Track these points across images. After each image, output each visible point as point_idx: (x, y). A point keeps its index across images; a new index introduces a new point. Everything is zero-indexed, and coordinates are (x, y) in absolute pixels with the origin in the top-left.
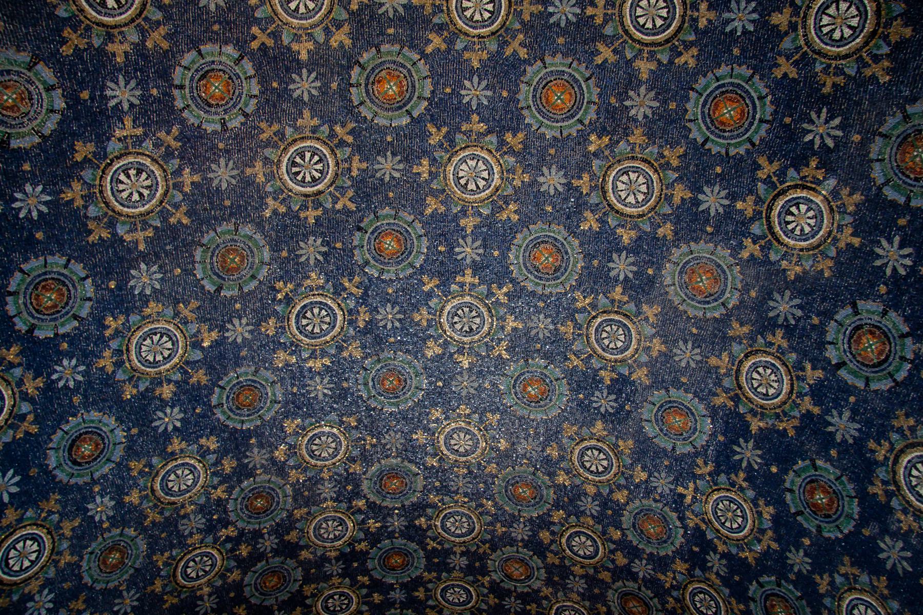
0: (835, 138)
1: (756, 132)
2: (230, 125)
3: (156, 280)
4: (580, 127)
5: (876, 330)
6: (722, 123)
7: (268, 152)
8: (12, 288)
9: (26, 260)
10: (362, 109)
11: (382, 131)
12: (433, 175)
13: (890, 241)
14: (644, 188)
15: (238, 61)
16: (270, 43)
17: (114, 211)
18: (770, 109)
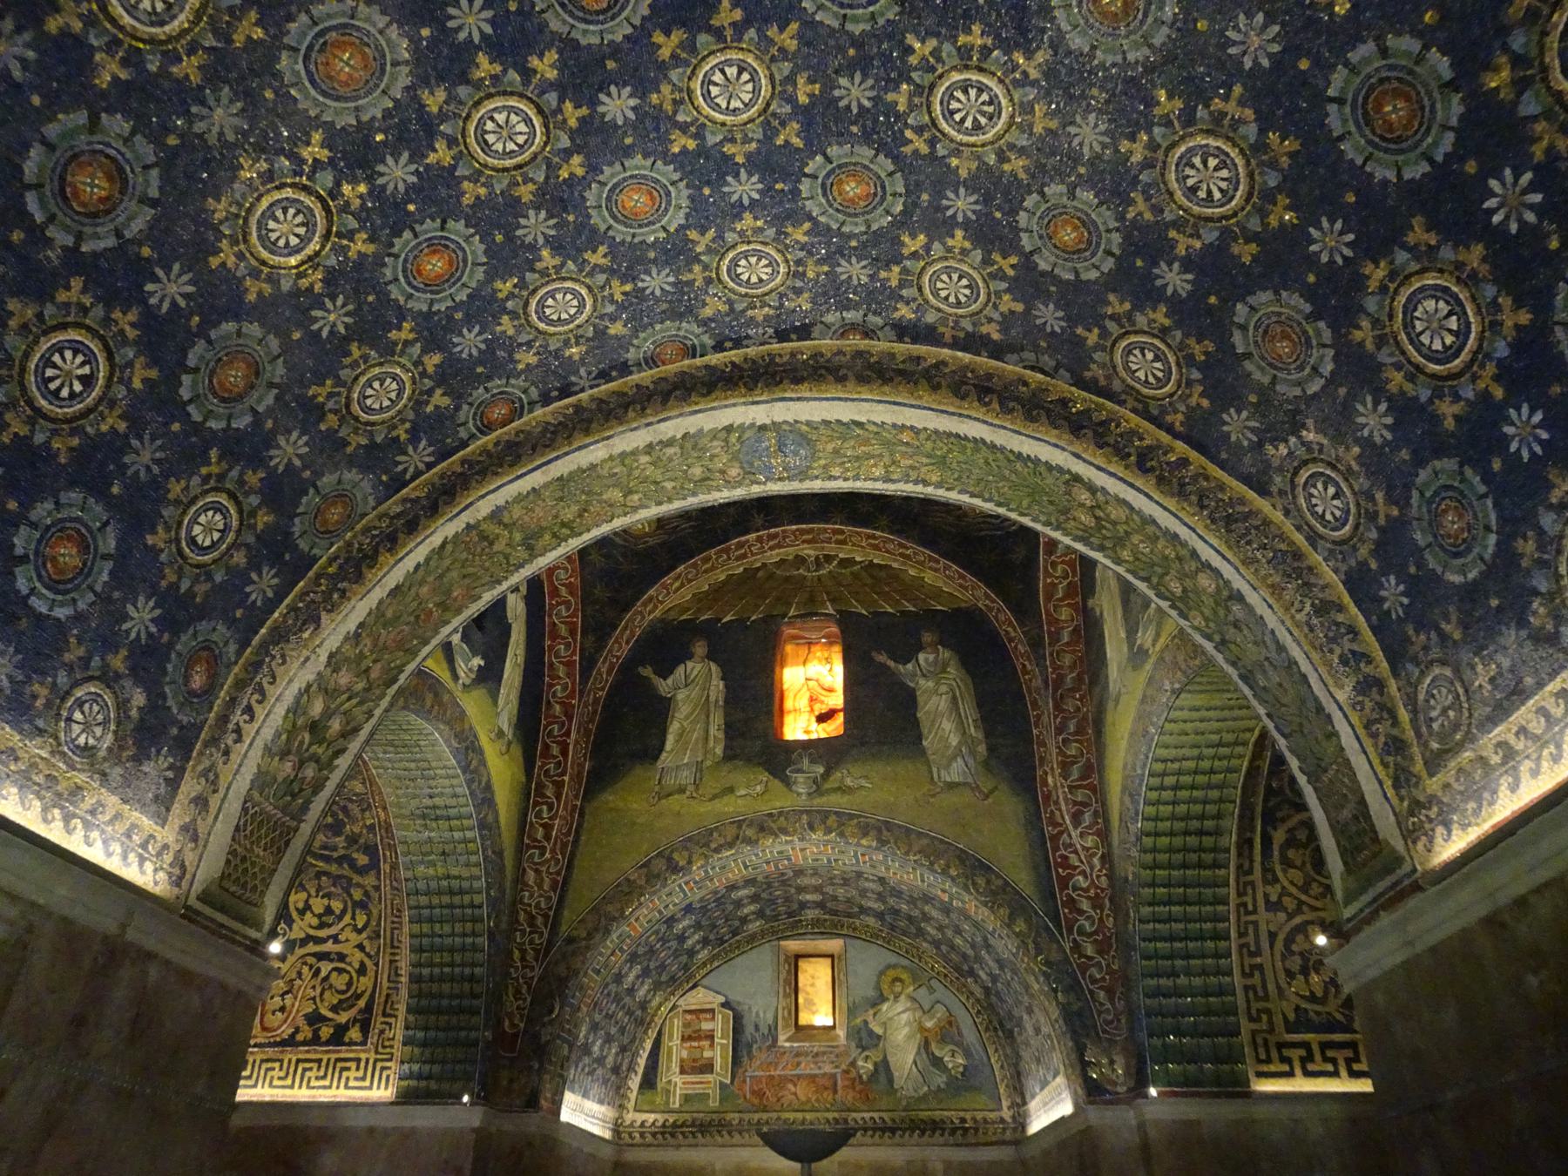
0: (316, 320)
1: (395, 268)
2: (1062, 188)
3: (1239, 31)
4: (601, 178)
5: (107, 207)
6: (434, 252)
7: (1023, 141)
8: (1425, 167)
9: (1385, 182)
10: (891, 168)
11: (866, 138)
12: (790, 80)
13: (185, 296)
14: (491, 138)
15: (1037, 251)
16: (996, 257)
17: (1248, 163)
18: (395, 293)
